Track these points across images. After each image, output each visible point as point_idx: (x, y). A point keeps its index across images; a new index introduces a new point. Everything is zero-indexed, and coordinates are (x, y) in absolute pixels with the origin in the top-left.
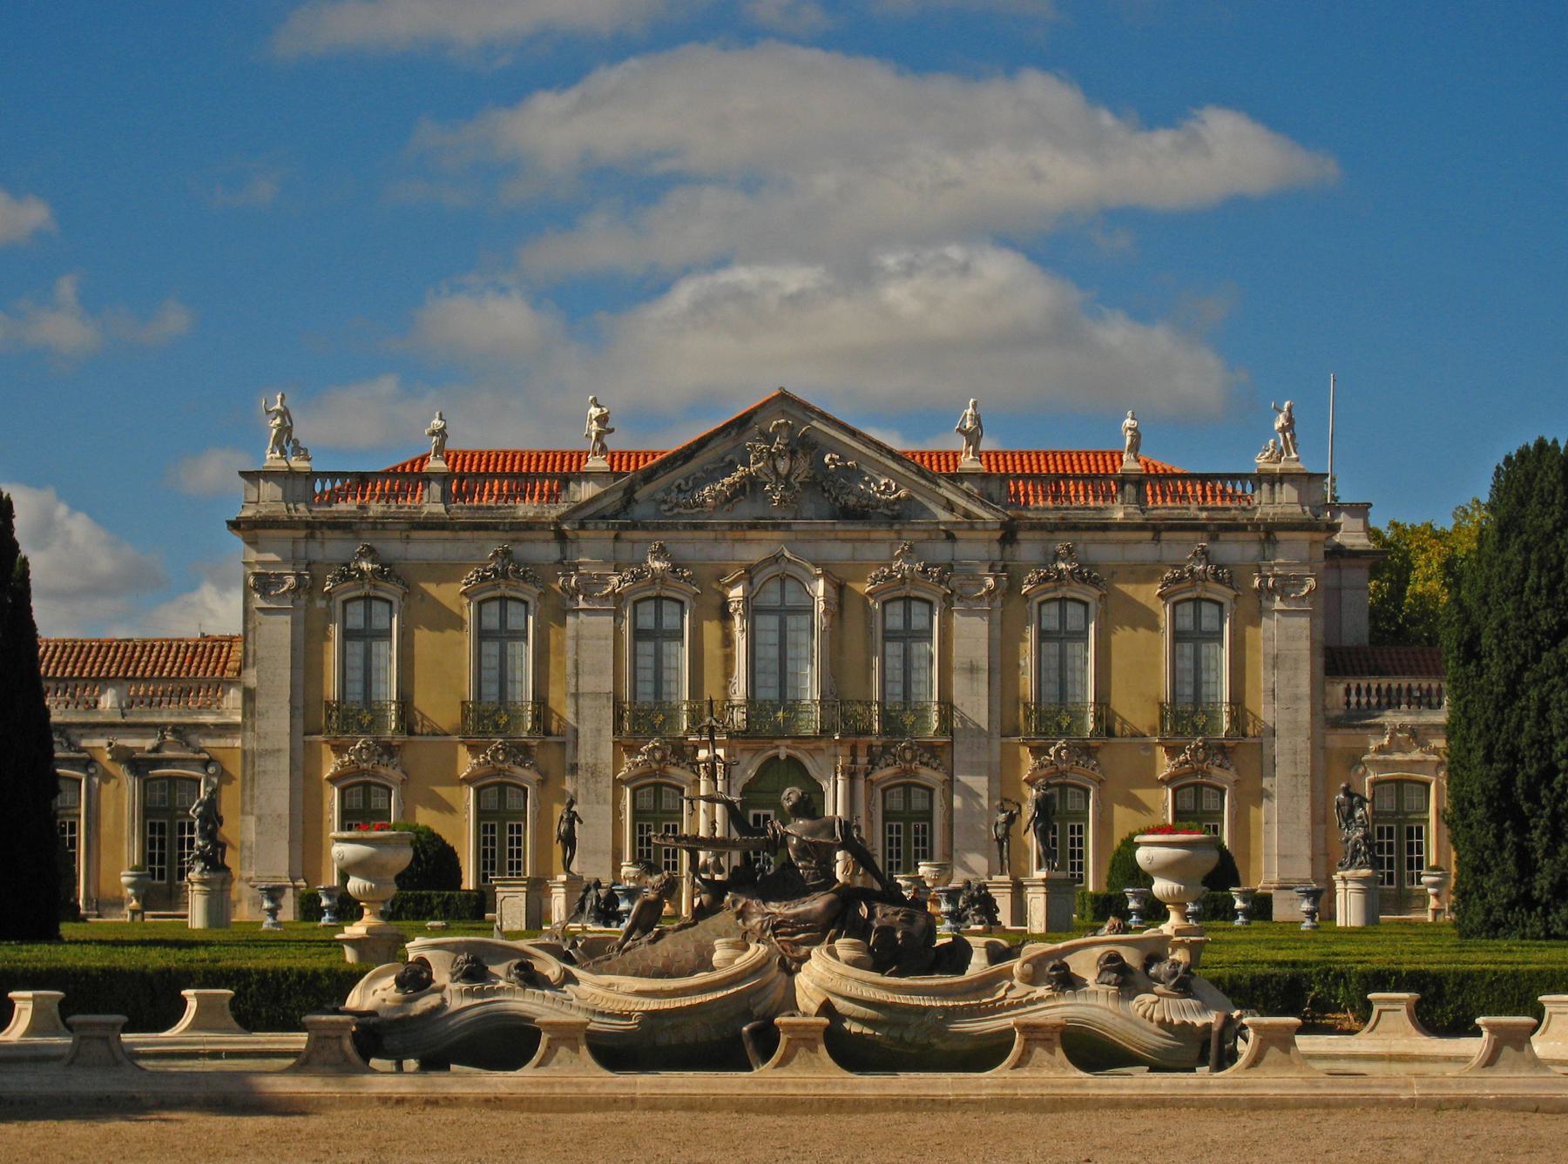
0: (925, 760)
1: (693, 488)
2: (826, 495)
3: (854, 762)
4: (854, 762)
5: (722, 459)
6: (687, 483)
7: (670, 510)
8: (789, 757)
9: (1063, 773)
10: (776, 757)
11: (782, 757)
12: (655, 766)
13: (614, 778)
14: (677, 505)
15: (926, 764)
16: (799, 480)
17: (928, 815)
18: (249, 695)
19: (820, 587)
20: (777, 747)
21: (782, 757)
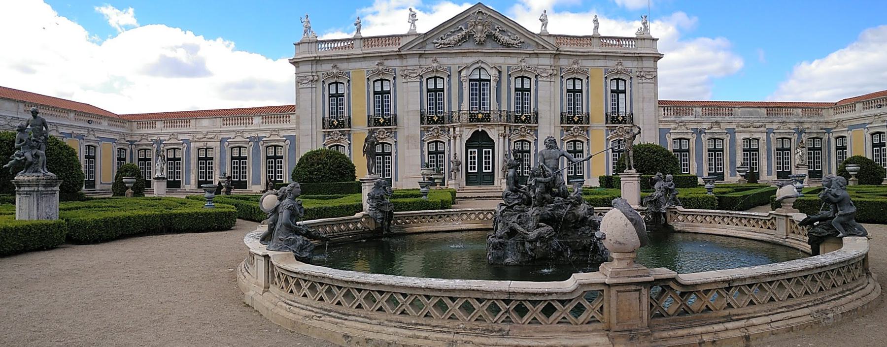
0: (528, 132)
1: (447, 38)
2: (496, 40)
3: (505, 132)
4: (505, 132)
5: (458, 28)
6: (444, 37)
7: (439, 46)
8: (482, 130)
9: (575, 137)
10: (478, 130)
11: (480, 130)
12: (435, 135)
13: (421, 140)
14: (441, 44)
15: (529, 133)
16: (486, 33)
17: (529, 152)
18: (298, 117)
19: (494, 72)
20: (478, 127)
21: (480, 130)
